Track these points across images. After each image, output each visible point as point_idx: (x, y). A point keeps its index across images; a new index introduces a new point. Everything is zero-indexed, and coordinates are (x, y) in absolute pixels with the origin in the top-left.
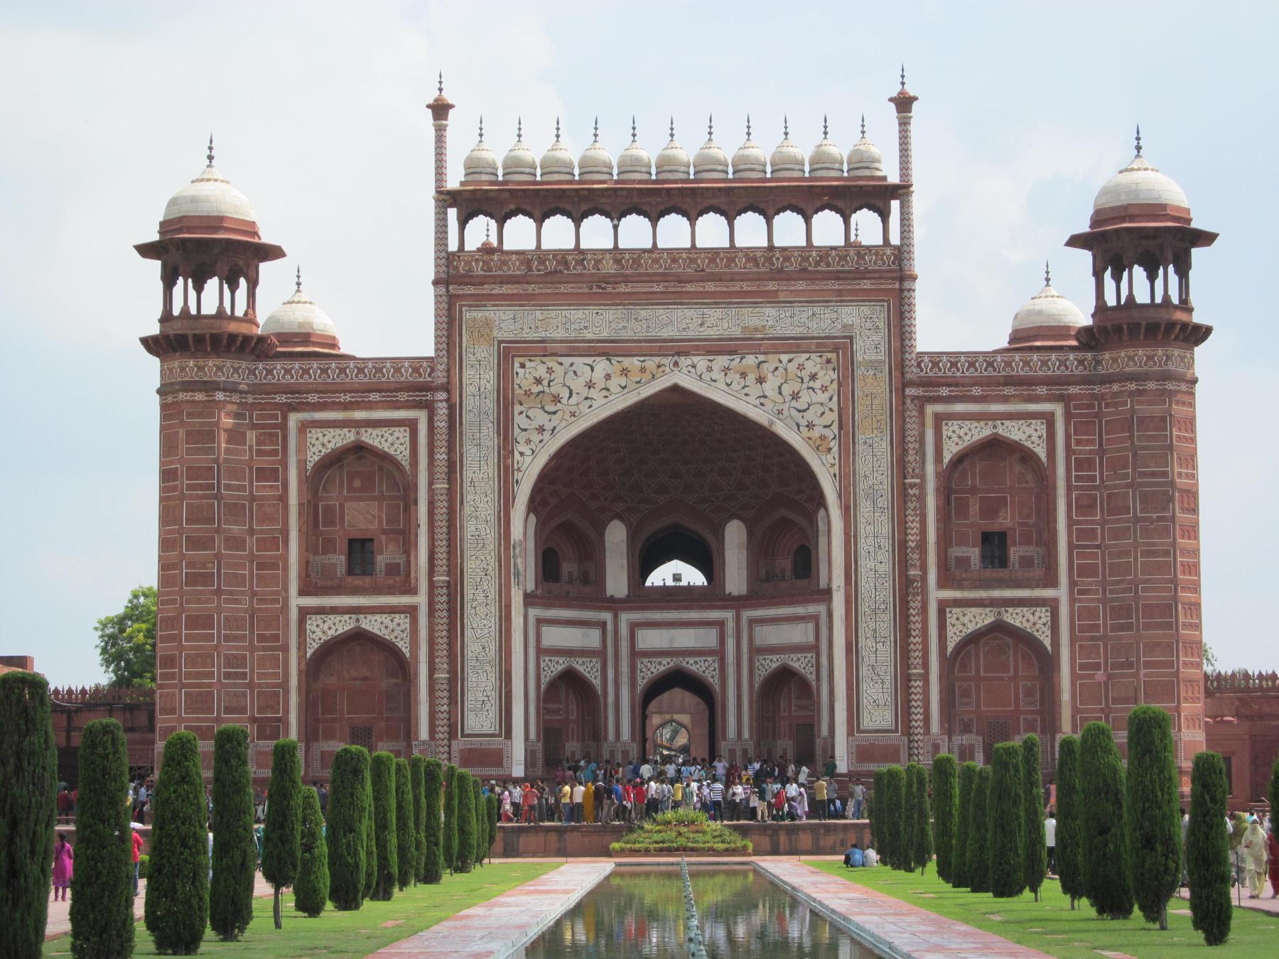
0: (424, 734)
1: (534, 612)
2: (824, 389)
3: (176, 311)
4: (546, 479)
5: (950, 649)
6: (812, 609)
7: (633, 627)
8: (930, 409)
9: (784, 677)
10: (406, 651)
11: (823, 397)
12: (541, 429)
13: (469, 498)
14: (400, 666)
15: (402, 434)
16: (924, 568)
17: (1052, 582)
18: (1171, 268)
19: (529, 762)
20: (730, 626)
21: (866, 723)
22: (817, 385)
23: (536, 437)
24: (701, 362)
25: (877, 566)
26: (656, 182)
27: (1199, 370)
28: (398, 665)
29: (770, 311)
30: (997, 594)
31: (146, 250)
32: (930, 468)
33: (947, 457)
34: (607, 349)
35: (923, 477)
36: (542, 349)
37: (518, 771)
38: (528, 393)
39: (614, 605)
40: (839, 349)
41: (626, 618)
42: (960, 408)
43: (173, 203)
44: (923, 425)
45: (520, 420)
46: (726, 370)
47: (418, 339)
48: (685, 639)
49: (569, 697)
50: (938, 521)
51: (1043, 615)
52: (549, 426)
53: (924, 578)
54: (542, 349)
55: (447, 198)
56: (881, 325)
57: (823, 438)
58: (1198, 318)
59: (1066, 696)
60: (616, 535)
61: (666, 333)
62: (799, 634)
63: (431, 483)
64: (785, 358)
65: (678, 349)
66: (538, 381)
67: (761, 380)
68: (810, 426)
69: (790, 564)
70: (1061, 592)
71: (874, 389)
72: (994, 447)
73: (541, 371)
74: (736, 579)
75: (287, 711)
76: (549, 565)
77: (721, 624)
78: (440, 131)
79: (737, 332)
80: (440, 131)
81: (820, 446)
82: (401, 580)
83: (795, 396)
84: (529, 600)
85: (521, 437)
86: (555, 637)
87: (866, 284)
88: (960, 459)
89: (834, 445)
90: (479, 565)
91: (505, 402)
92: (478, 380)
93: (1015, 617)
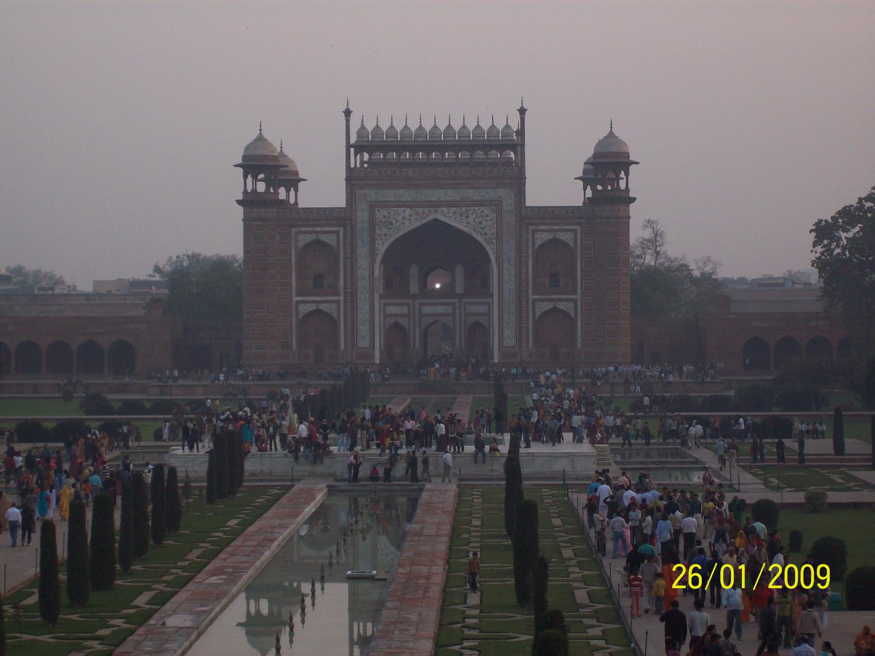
0: (342, 348)
1: (382, 301)
2: (491, 220)
3: (249, 190)
4: (386, 251)
5: (537, 316)
6: (489, 300)
7: (421, 305)
8: (531, 228)
9: (477, 326)
10: (336, 317)
11: (490, 223)
12: (385, 235)
13: (359, 261)
14: (333, 323)
15: (334, 236)
16: (528, 287)
17: (575, 292)
18: (622, 175)
19: (381, 358)
20: (457, 305)
21: (505, 344)
22: (488, 219)
23: (383, 238)
24: (445, 210)
25: (510, 286)
26: (430, 141)
27: (631, 214)
29: (471, 191)
30: (554, 297)
31: (235, 166)
32: (530, 250)
33: (537, 245)
34: (412, 205)
35: (527, 253)
36: (386, 205)
37: (377, 361)
38: (381, 221)
39: (414, 297)
40: (497, 205)
41: (417, 302)
42: (541, 227)
43: (247, 148)
44: (528, 233)
45: (378, 231)
46: (454, 213)
49: (396, 332)
50: (533, 269)
51: (571, 304)
52: (388, 234)
53: (527, 292)
54: (386, 205)
55: (348, 146)
56: (513, 196)
57: (490, 238)
58: (631, 195)
59: (579, 335)
60: (414, 271)
61: (434, 199)
62: (482, 309)
63: (345, 254)
64: (476, 208)
65: (437, 205)
66: (385, 217)
67: (467, 217)
68: (486, 234)
72: (555, 242)
73: (386, 213)
74: (459, 289)
75: (292, 339)
76: (388, 282)
77: (453, 304)
78: (348, 121)
79: (458, 198)
80: (348, 121)
83: (480, 223)
84: (381, 297)
85: (378, 238)
86: (391, 310)
87: (507, 181)
88: (543, 245)
89: (495, 241)
90: (362, 285)
92: (362, 216)
93: (561, 306)
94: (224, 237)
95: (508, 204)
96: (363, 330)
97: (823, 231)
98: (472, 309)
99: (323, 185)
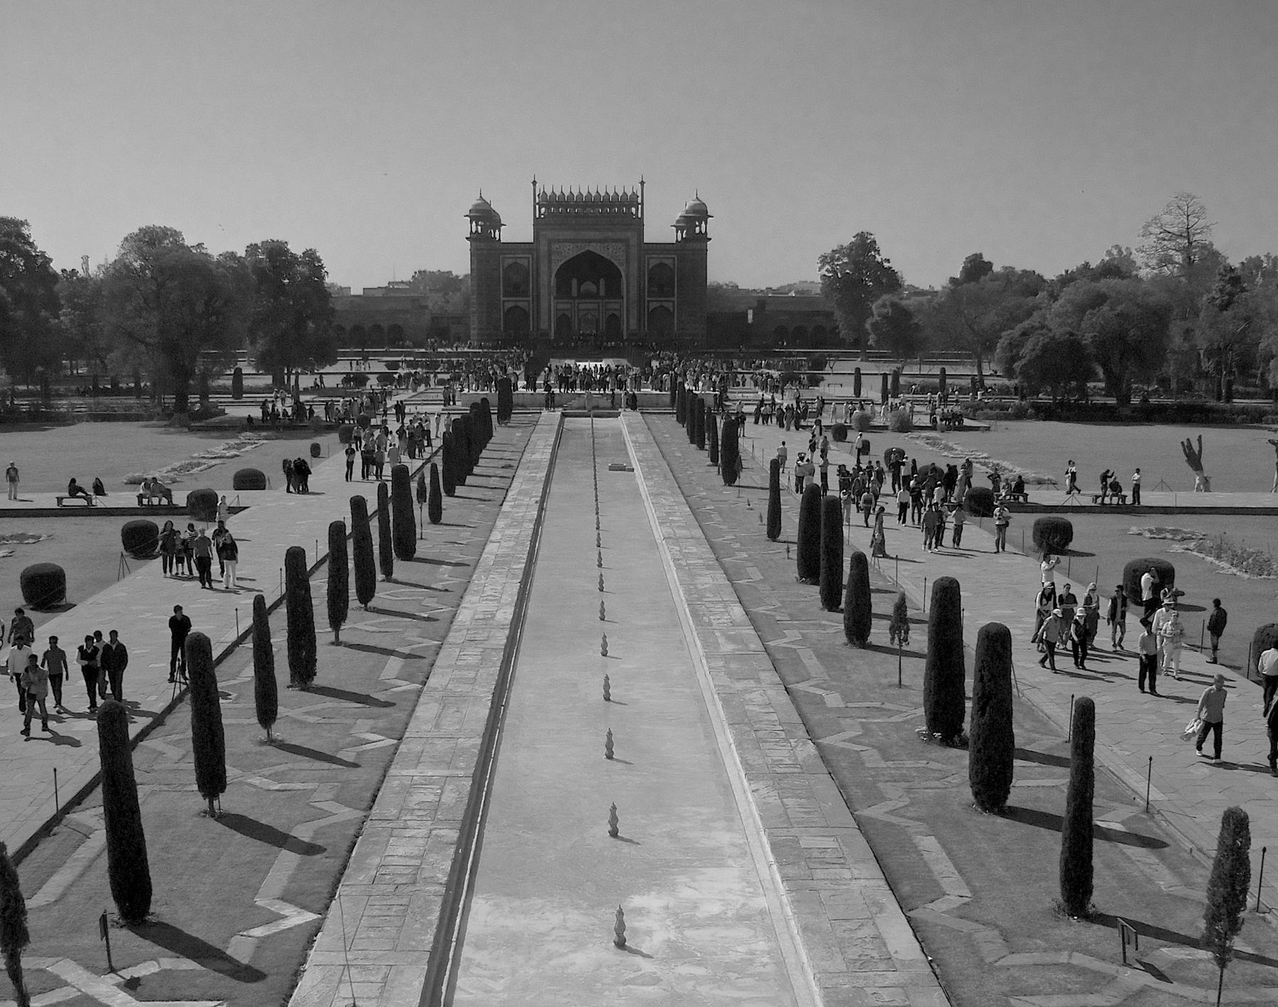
25: (634, 292)
28: (526, 314)
36: (559, 241)
39: (574, 298)
40: (626, 242)
47: (528, 237)
48: (590, 306)
49: (563, 321)
54: (559, 241)
60: (574, 282)
62: (617, 306)
65: (590, 241)
69: (614, 290)
70: (675, 299)
71: (634, 251)
72: (661, 265)
74: (602, 293)
76: (559, 289)
81: (622, 264)
82: (525, 293)
86: (561, 306)
90: (544, 291)
91: (550, 253)
92: (544, 248)
93: (665, 304)
94: (459, 263)
95: (634, 241)
96: (544, 317)
97: (824, 260)
98: (609, 306)
99: (517, 227)
